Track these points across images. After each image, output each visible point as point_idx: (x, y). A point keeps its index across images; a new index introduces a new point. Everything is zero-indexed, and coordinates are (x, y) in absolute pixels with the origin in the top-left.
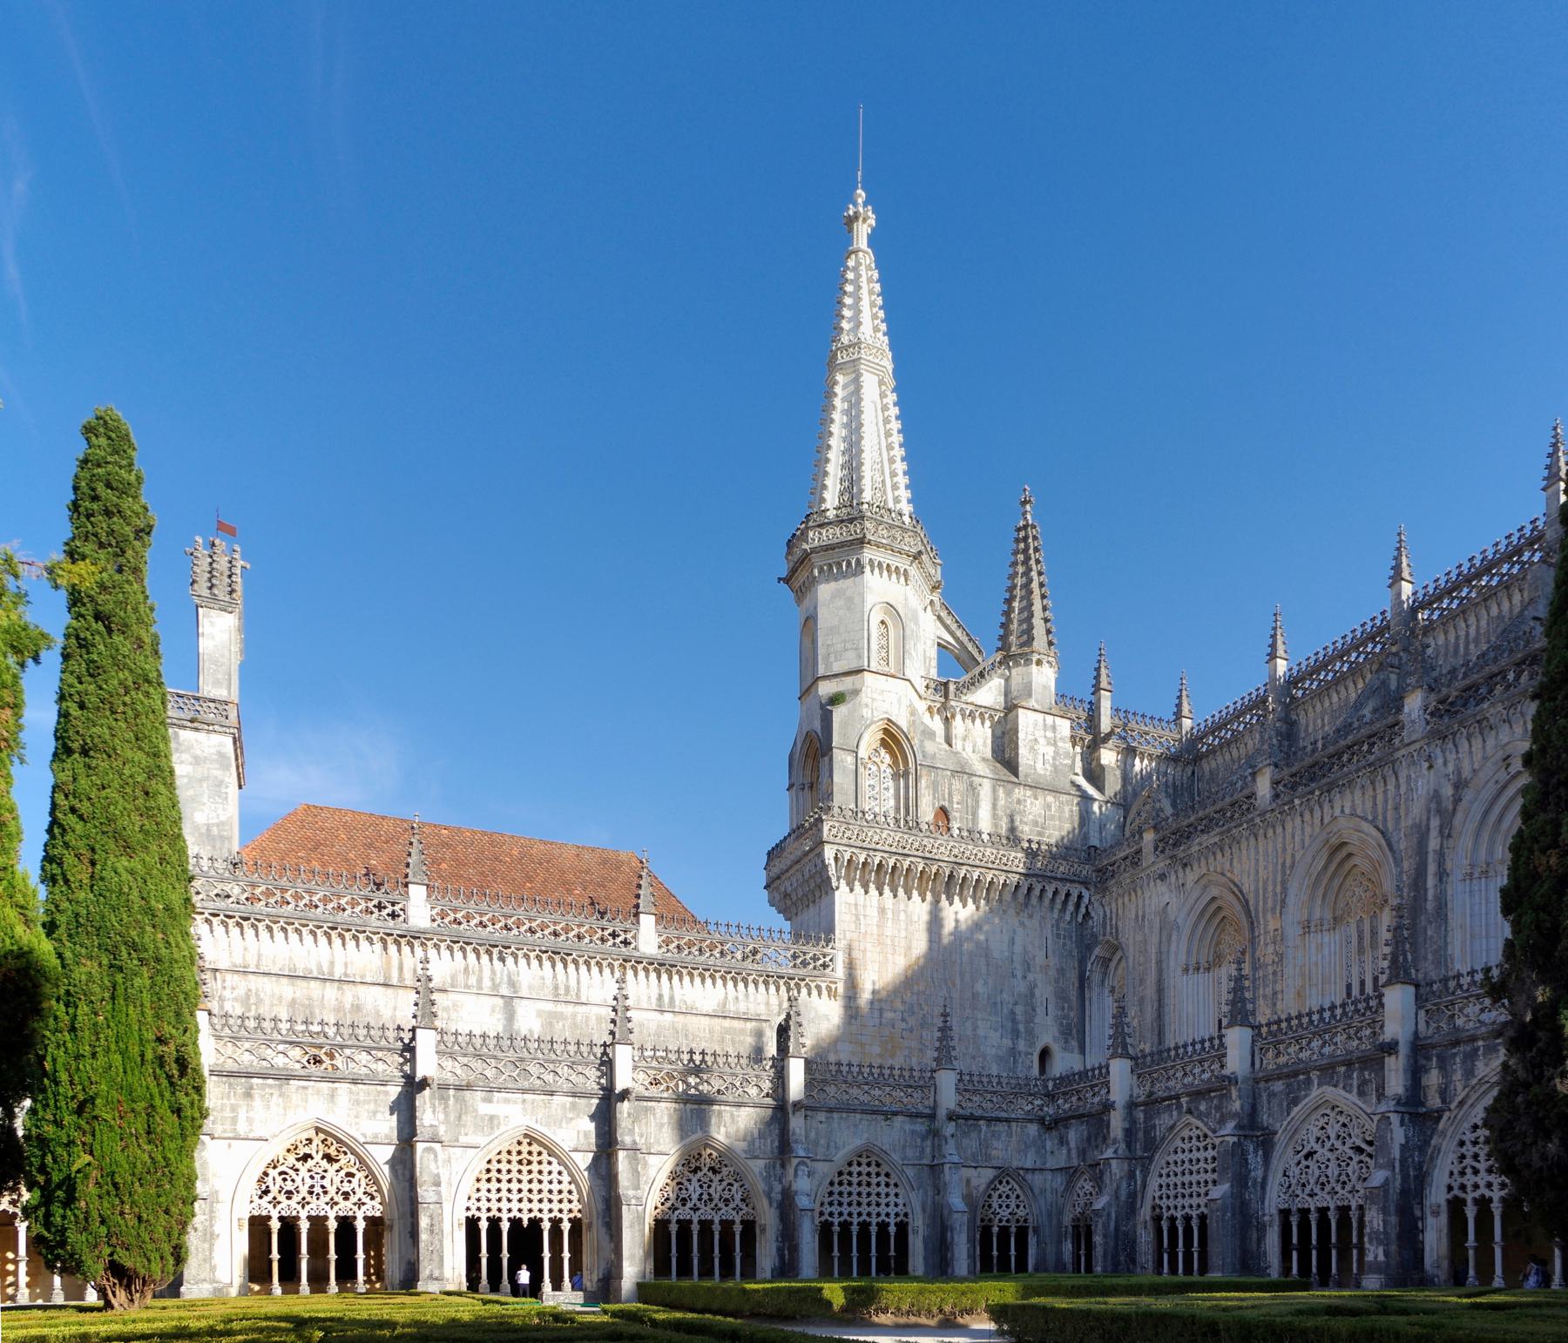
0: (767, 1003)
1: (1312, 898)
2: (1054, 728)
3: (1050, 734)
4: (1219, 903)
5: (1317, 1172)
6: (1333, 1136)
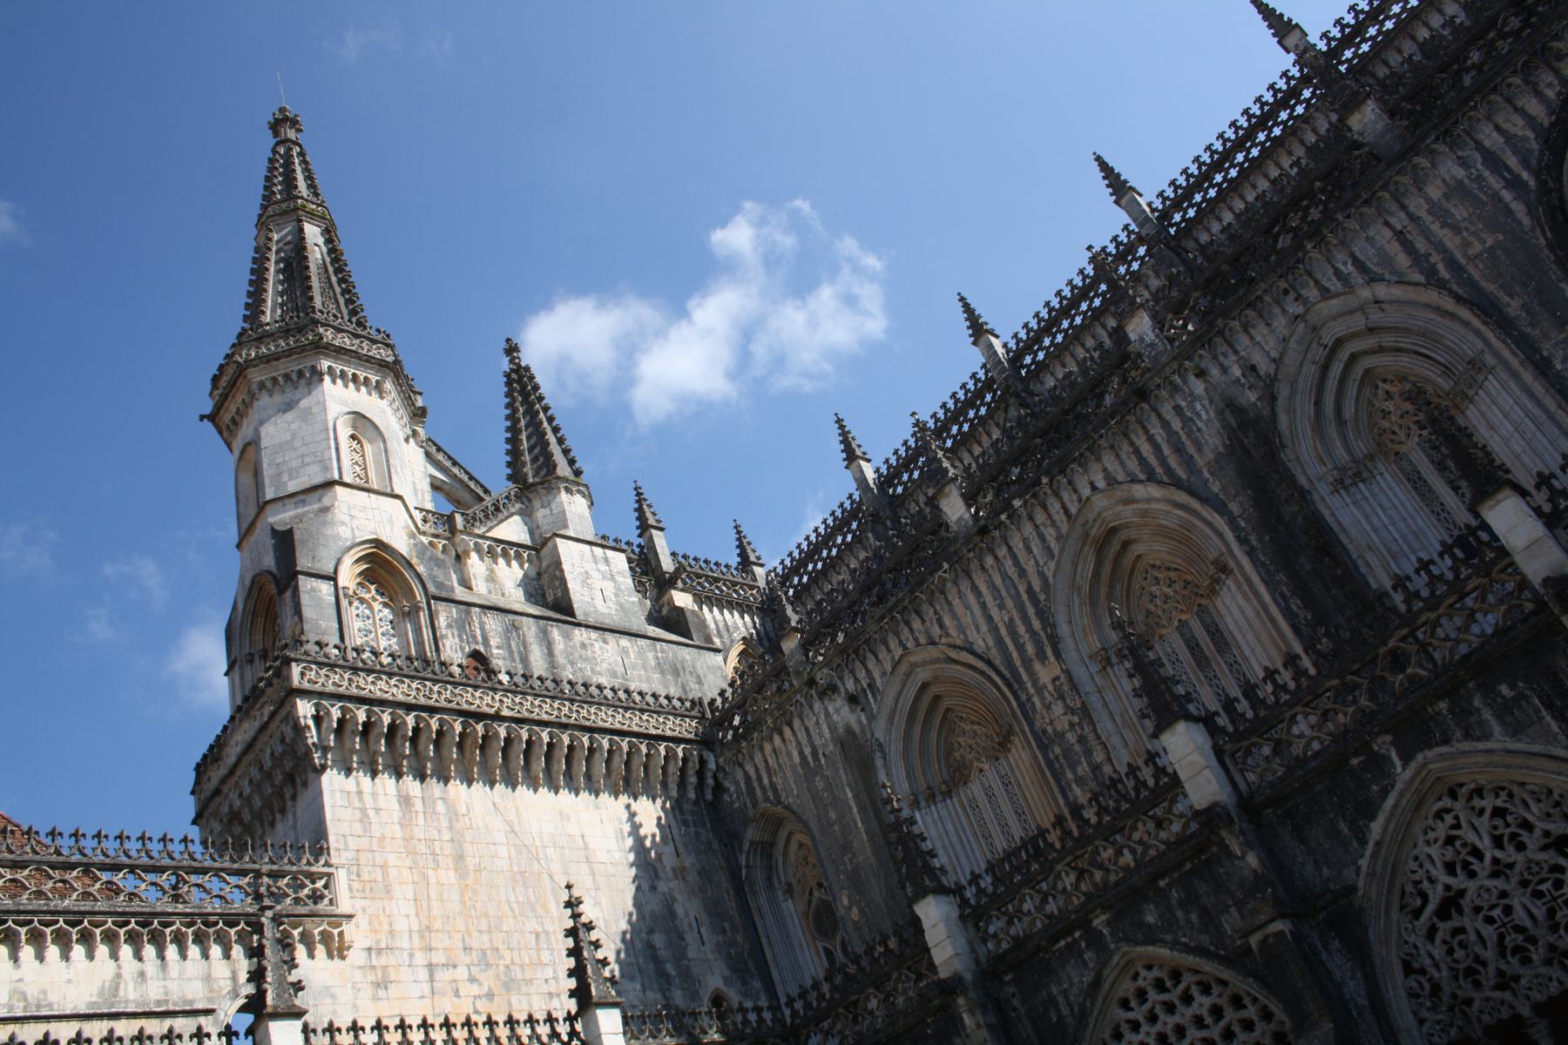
0: (208, 978)
2: (606, 560)
3: (603, 567)
4: (935, 690)
5: (1488, 931)
6: (1485, 844)
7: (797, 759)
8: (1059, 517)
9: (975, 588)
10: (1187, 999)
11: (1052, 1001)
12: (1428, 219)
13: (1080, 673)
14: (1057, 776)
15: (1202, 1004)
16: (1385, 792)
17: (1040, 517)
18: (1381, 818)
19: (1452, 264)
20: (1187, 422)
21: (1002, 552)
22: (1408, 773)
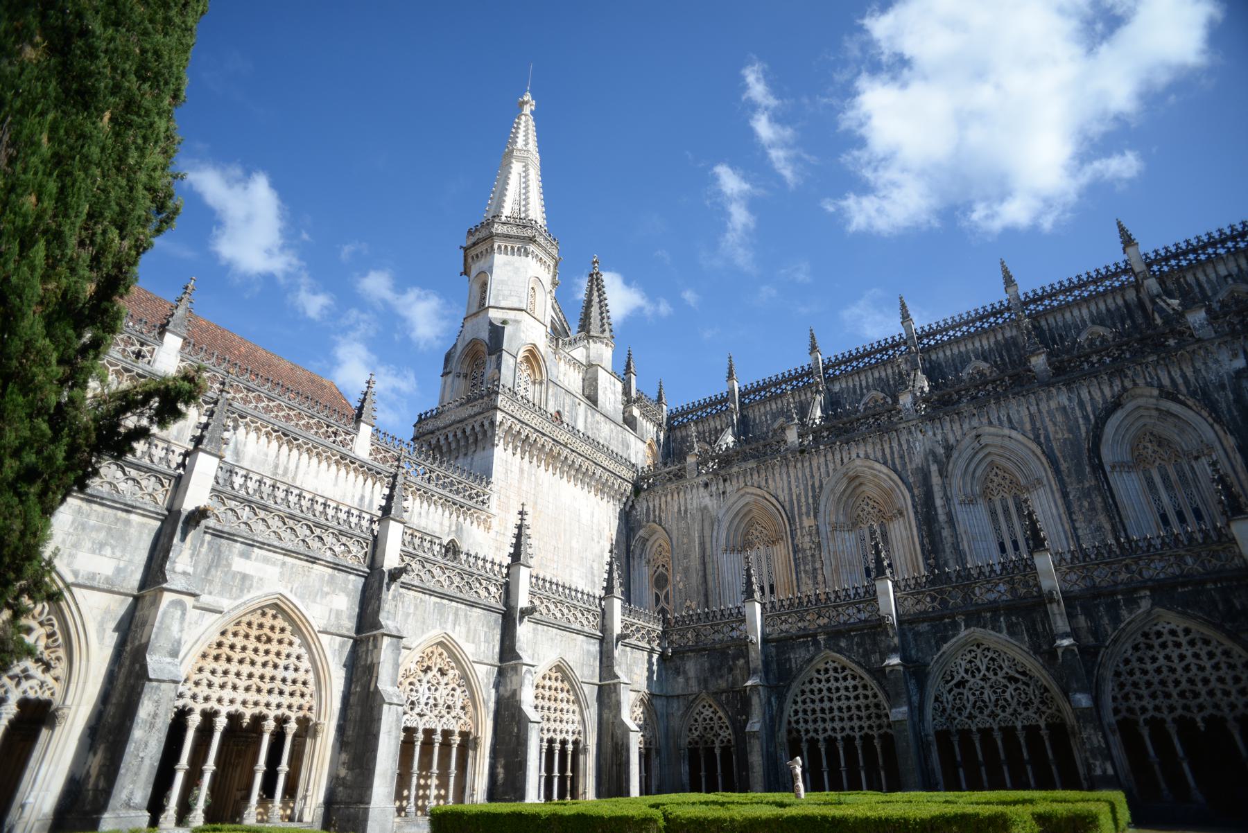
0: (441, 524)
1: (837, 511)
5: (972, 698)
6: (983, 668)
7: (676, 509)
8: (838, 461)
9: (788, 473)
10: (845, 679)
11: (789, 659)
12: (1045, 415)
13: (822, 528)
14: (797, 566)
15: (850, 683)
16: (954, 636)
17: (830, 457)
18: (949, 644)
19: (1047, 437)
20: (909, 447)
21: (807, 464)
22: (967, 632)
